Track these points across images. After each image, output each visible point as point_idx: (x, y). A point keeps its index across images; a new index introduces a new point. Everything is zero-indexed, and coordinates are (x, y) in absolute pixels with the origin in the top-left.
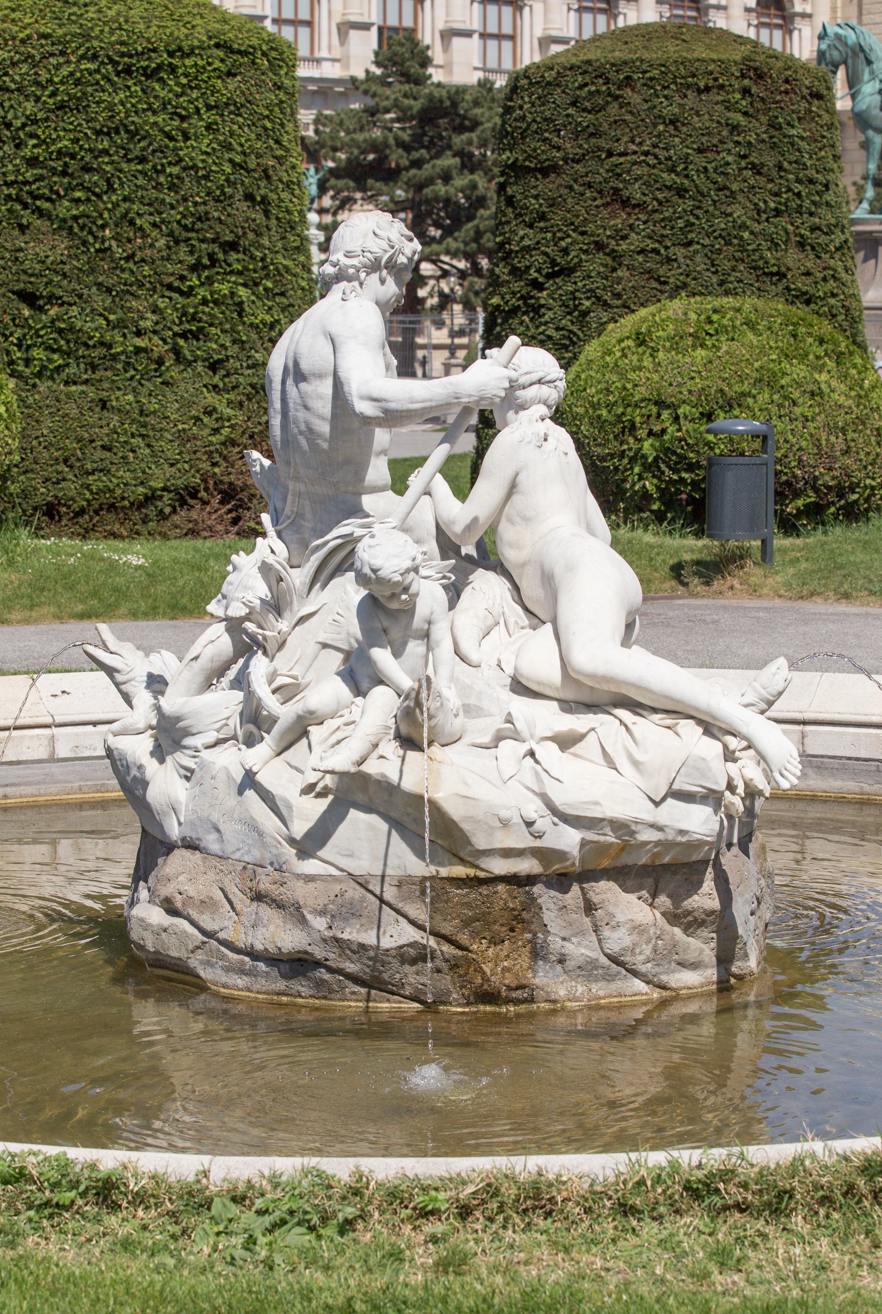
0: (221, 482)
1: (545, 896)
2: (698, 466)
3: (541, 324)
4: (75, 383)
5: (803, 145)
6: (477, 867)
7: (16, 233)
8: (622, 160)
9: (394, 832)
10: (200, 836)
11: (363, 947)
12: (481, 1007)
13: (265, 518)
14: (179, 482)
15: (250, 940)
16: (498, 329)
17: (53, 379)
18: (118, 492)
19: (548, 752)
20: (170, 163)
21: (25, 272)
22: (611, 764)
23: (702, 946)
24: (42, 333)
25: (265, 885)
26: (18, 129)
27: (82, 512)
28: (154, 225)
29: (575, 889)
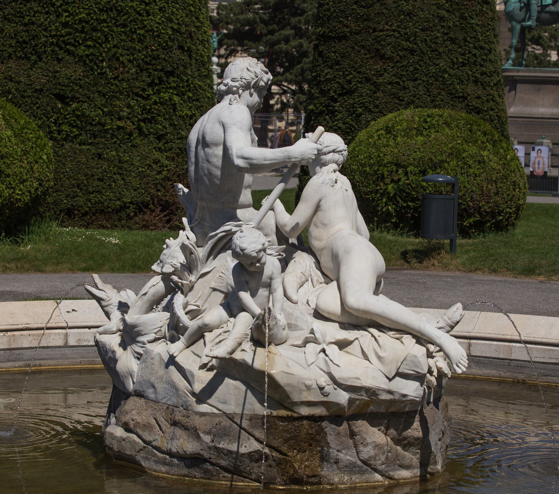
0: (161, 200)
1: (329, 428)
2: (417, 199)
3: (335, 120)
4: (84, 144)
5: (478, 28)
6: (293, 411)
7: (55, 62)
8: (381, 34)
9: (249, 391)
10: (144, 389)
11: (230, 452)
12: (293, 487)
13: (185, 220)
14: (139, 199)
15: (169, 446)
16: (312, 122)
17: (73, 142)
18: (106, 204)
19: (333, 350)
20: (139, 28)
21: (59, 84)
22: (365, 357)
23: (412, 457)
24: (68, 117)
25: (178, 417)
26: (58, 7)
27: (86, 214)
28: (130, 61)
29: (345, 425)
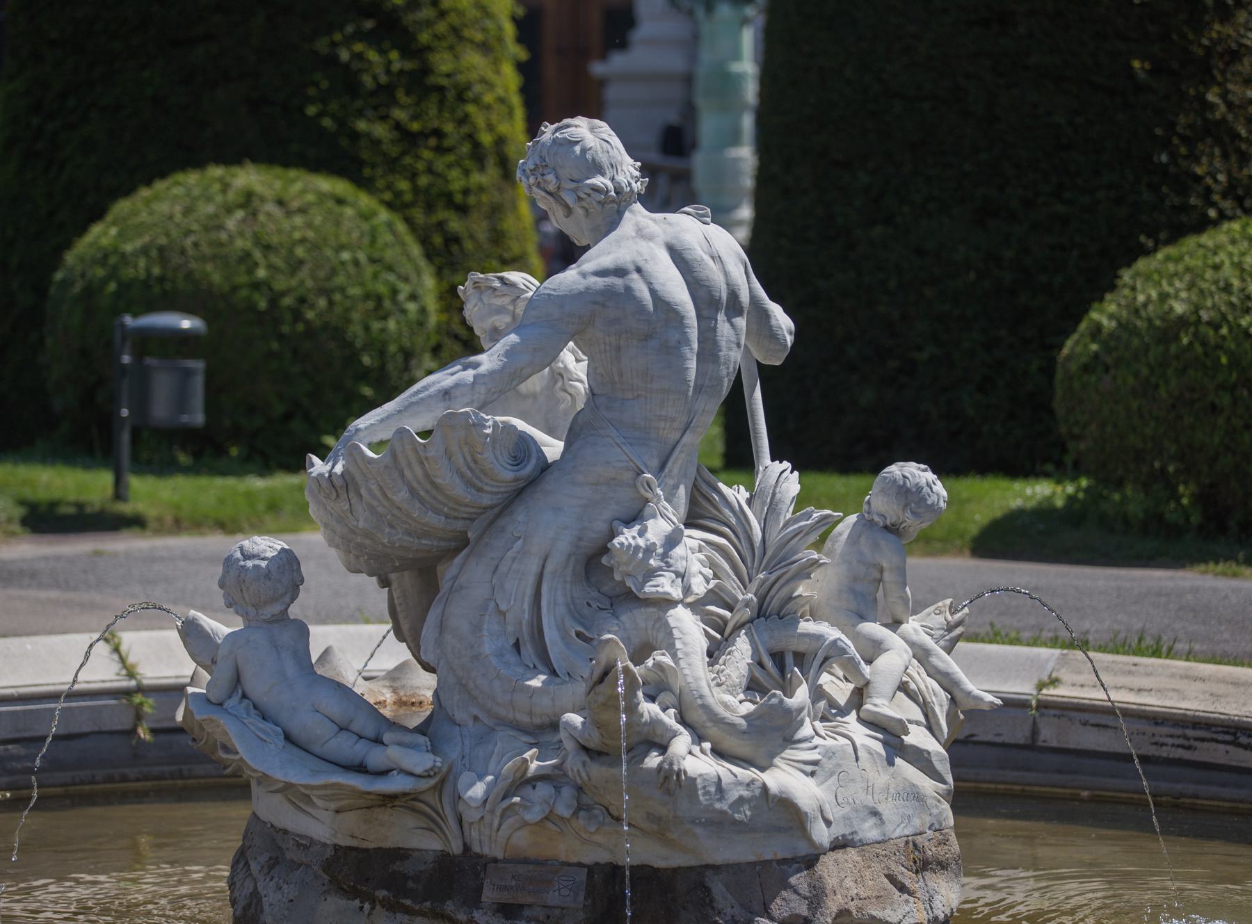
10: (856, 828)
